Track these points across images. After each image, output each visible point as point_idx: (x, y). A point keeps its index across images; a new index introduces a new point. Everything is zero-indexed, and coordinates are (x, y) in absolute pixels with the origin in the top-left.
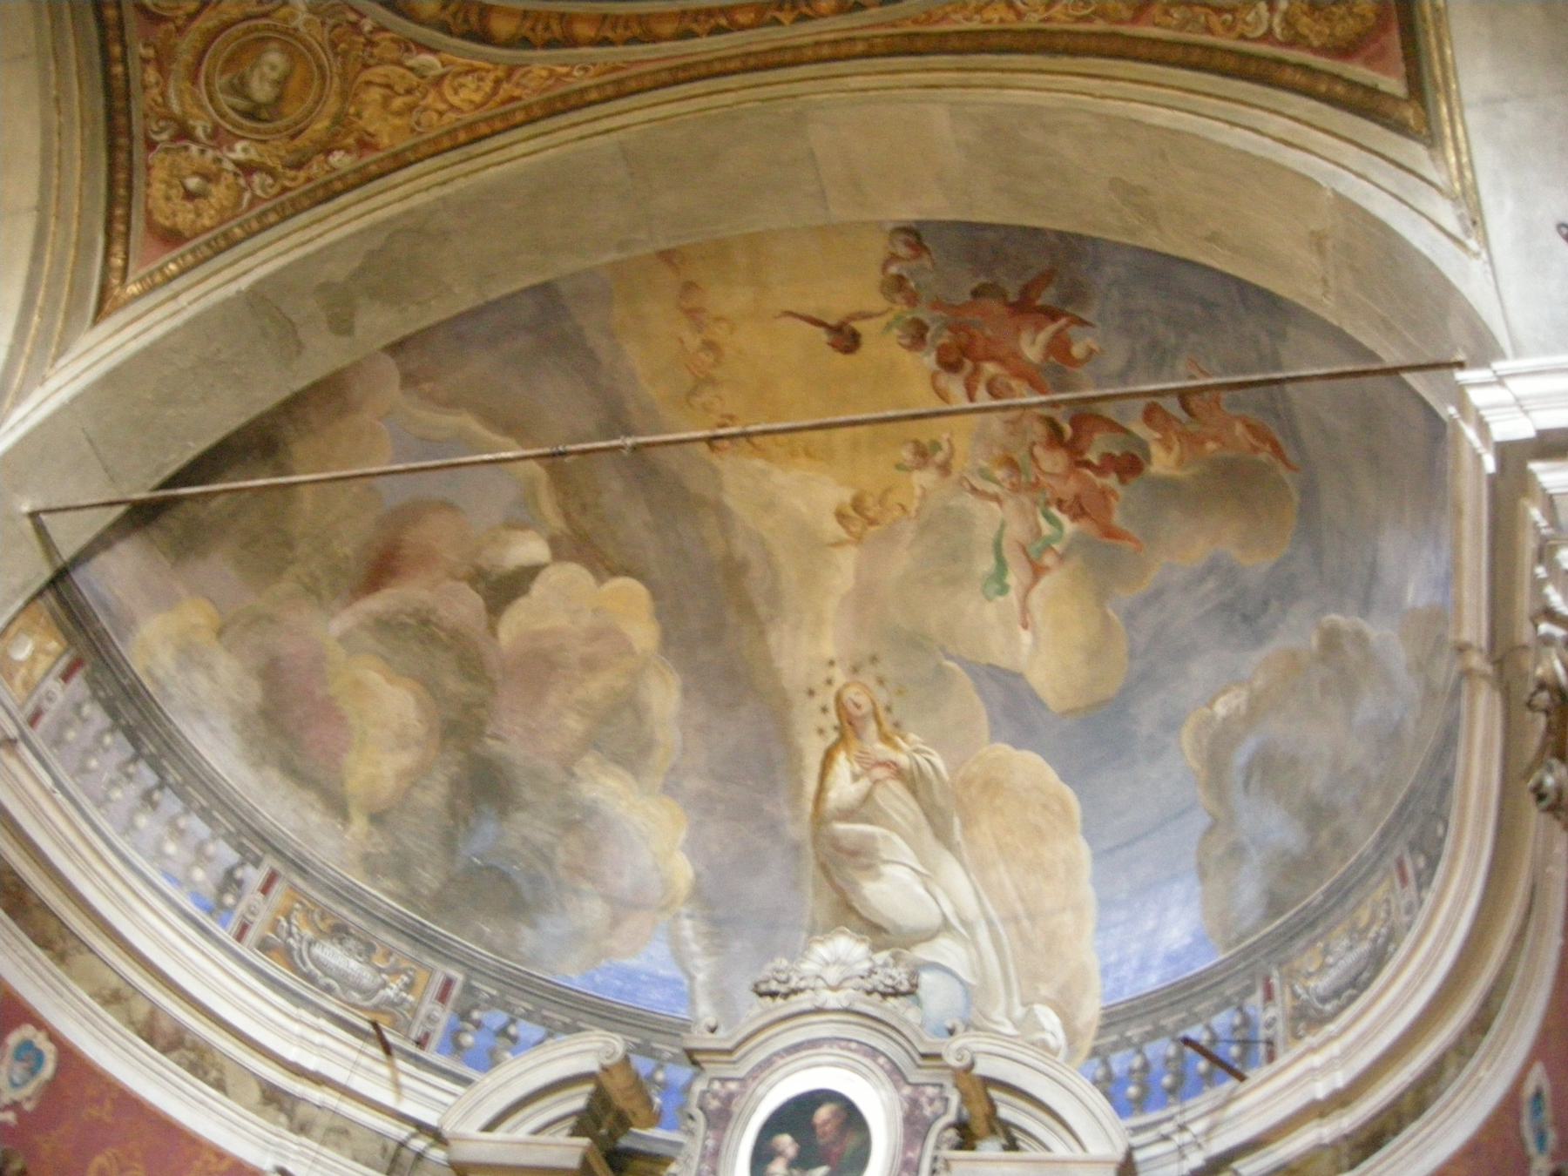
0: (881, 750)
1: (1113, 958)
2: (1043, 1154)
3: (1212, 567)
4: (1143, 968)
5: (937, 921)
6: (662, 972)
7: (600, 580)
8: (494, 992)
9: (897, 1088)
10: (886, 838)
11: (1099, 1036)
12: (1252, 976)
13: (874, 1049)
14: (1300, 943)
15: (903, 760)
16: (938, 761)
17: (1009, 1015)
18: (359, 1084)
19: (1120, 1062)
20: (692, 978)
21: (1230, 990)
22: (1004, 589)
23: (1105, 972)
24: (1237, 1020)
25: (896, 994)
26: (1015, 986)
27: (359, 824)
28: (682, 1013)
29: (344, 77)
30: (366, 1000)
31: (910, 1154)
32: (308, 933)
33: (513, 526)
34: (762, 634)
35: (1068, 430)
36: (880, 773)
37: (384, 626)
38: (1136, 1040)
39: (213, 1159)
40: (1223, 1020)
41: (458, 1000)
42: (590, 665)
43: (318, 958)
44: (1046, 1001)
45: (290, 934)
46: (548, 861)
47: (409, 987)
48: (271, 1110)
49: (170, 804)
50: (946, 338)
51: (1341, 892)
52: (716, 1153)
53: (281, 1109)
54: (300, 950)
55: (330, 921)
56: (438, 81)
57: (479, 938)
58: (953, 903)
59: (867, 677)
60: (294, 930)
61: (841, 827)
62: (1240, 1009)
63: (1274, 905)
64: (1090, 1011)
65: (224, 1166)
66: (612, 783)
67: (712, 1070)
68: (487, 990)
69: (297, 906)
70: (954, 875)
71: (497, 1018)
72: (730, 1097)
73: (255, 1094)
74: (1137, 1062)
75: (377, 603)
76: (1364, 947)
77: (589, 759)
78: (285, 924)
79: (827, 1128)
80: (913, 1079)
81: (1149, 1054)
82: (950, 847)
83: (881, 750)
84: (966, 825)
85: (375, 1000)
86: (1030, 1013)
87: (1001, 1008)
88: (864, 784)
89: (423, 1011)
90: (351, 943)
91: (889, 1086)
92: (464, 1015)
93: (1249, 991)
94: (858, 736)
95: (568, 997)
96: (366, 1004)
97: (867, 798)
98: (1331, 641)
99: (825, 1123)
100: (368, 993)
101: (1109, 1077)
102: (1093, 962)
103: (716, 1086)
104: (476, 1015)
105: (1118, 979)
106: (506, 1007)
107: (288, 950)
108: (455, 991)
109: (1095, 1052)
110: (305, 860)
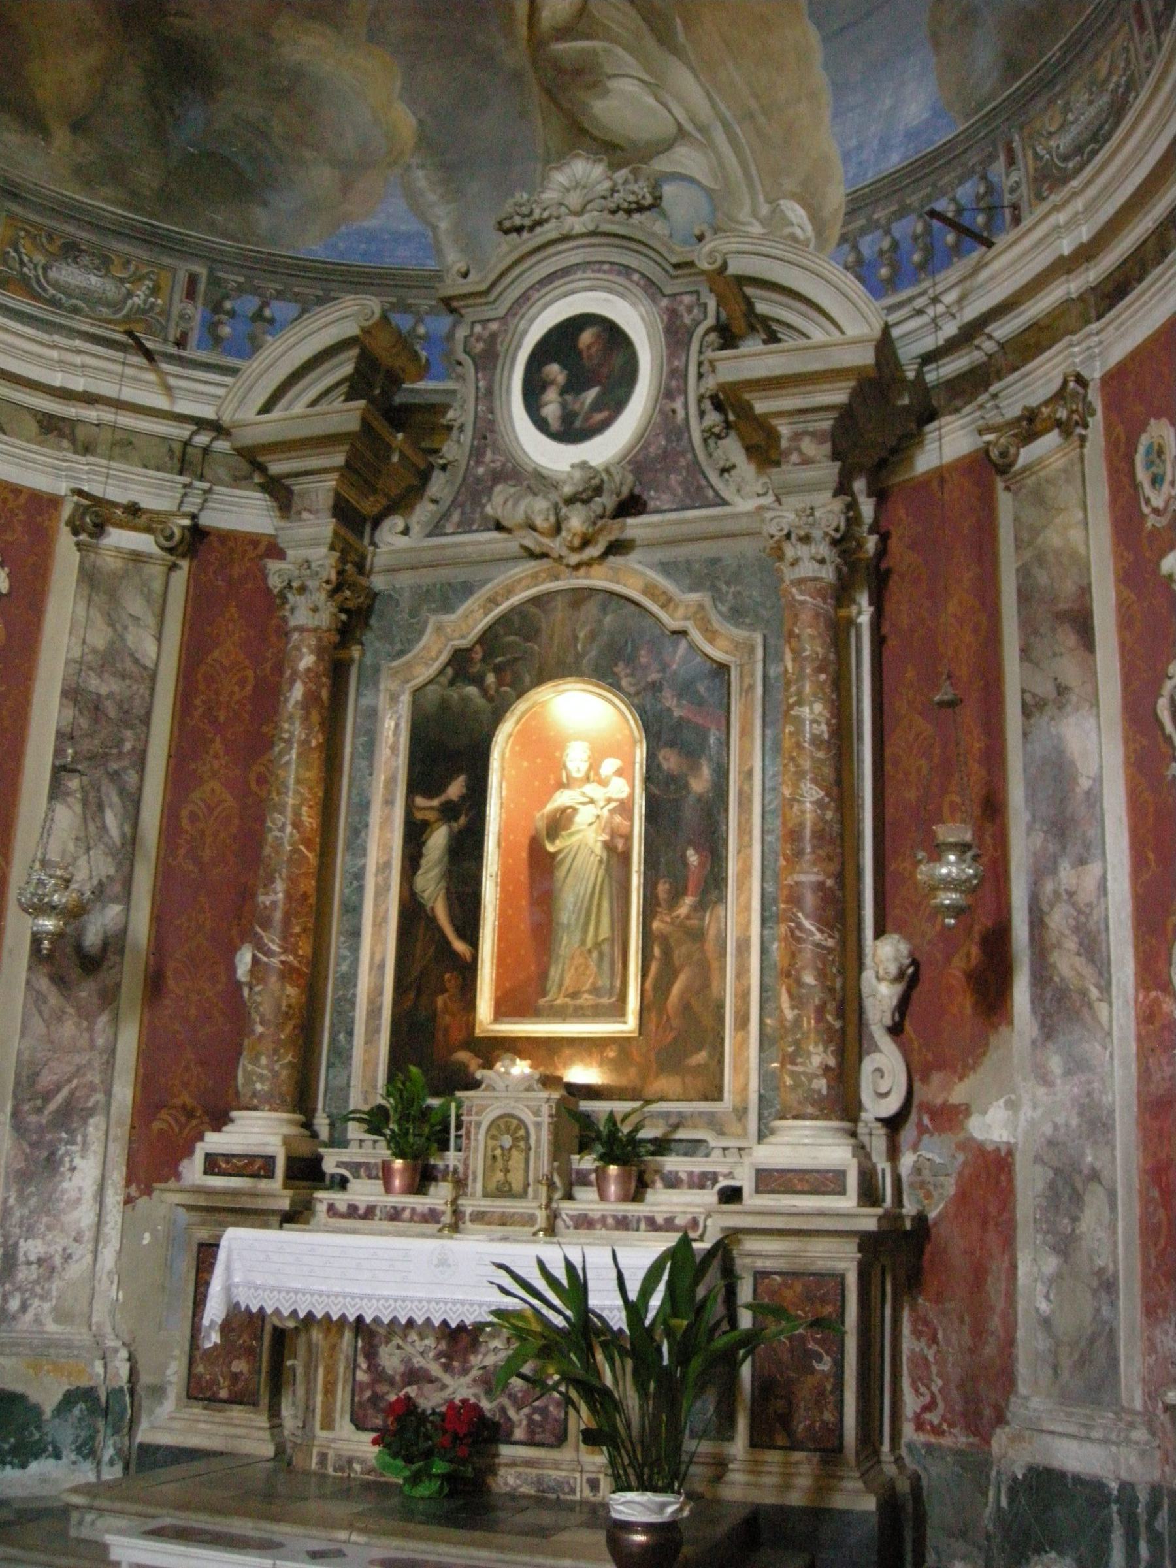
1: (854, 143)
2: (803, 342)
4: (885, 148)
5: (673, 129)
6: (403, 227)
8: (241, 279)
9: (654, 300)
10: (605, 50)
11: (846, 223)
12: (994, 144)
13: (627, 267)
17: (754, 214)
18: (129, 394)
19: (869, 245)
20: (435, 228)
21: (973, 158)
23: (846, 157)
24: (982, 190)
25: (641, 209)
26: (759, 187)
27: (62, 137)
28: (432, 264)
30: (115, 313)
31: (676, 363)
32: (40, 259)
38: (883, 221)
39: (11, 496)
41: (206, 294)
43: (57, 281)
44: (793, 196)
45: (22, 263)
46: (264, 136)
47: (155, 291)
48: (51, 437)
52: (490, 392)
53: (62, 435)
54: (37, 278)
55: (59, 242)
57: (212, 226)
58: (687, 110)
60: (26, 259)
62: (984, 178)
63: (1011, 66)
64: (836, 197)
65: (22, 500)
66: (313, 41)
67: (470, 314)
68: (234, 279)
69: (22, 234)
70: (685, 81)
71: (250, 304)
72: (494, 336)
73: (33, 427)
74: (886, 244)
78: (13, 254)
79: (593, 350)
80: (667, 291)
81: (897, 235)
82: (675, 50)
84: (687, 26)
85: (124, 312)
86: (775, 210)
87: (747, 209)
89: (175, 311)
91: (647, 301)
92: (217, 308)
93: (992, 158)
95: (316, 270)
96: (117, 316)
99: (589, 347)
100: (116, 306)
101: (860, 261)
102: (834, 152)
103: (478, 328)
104: (228, 305)
105: (860, 163)
106: (257, 291)
107: (25, 279)
108: (202, 287)
109: (843, 239)
110: (17, 185)
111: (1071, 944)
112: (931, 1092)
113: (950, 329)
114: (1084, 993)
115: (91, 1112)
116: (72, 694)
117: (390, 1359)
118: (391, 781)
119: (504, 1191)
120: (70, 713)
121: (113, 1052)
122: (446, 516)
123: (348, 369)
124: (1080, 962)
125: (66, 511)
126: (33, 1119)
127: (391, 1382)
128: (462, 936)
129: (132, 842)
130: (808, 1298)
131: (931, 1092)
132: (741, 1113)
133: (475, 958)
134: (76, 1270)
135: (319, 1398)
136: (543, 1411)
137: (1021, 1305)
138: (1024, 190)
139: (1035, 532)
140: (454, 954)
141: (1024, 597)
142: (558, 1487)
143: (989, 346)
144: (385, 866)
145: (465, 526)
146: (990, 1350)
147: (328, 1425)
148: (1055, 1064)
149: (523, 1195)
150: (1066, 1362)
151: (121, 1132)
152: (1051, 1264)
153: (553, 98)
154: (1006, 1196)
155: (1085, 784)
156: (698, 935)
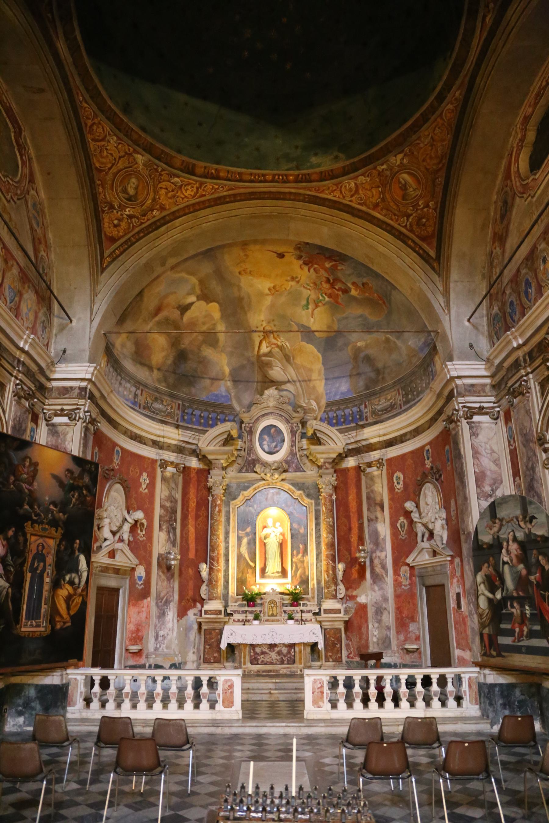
0: (274, 341)
3: (361, 316)
4: (336, 394)
7: (208, 304)
14: (373, 397)
15: (279, 344)
16: (288, 344)
17: (304, 401)
19: (331, 414)
22: (308, 309)
23: (327, 394)
27: (156, 371)
28: (229, 403)
29: (154, 186)
33: (189, 294)
34: (246, 314)
35: (332, 281)
36: (273, 346)
37: (159, 323)
40: (355, 409)
42: (204, 323)
49: (123, 382)
50: (307, 259)
51: (382, 390)
52: (251, 440)
56: (181, 187)
59: (272, 324)
61: (264, 358)
63: (367, 387)
64: (323, 402)
68: (187, 404)
70: (291, 370)
72: (251, 427)
73: (151, 443)
74: (335, 415)
75: (157, 319)
76: (389, 403)
77: (204, 346)
82: (290, 363)
83: (274, 341)
86: (309, 402)
88: (269, 349)
90: (159, 401)
92: (184, 412)
93: (361, 404)
94: (268, 337)
97: (270, 352)
98: (387, 340)
100: (164, 412)
106: (192, 408)
109: (325, 412)
111: (379, 566)
112: (350, 593)
113: (353, 440)
114: (382, 575)
115: (171, 601)
116: (162, 506)
117: (258, 650)
118: (234, 528)
119: (272, 615)
120: (162, 511)
121: (173, 588)
122: (242, 468)
123: (226, 436)
124: (382, 570)
125: (159, 463)
126: (160, 604)
127: (258, 654)
128: (252, 561)
129: (175, 540)
130: (335, 633)
131: (350, 593)
132: (313, 598)
133: (255, 566)
134: (169, 637)
135: (242, 660)
136: (290, 658)
137: (370, 633)
138: (368, 413)
139: (371, 486)
140: (250, 566)
141: (368, 498)
142: (294, 672)
143: (360, 445)
144: (233, 546)
145: (247, 471)
146: (363, 642)
147: (245, 664)
148: (376, 588)
149: (276, 616)
150: (380, 642)
151: (176, 605)
152: (376, 625)
153: (260, 368)
154: (366, 613)
155: (382, 537)
156: (303, 562)
